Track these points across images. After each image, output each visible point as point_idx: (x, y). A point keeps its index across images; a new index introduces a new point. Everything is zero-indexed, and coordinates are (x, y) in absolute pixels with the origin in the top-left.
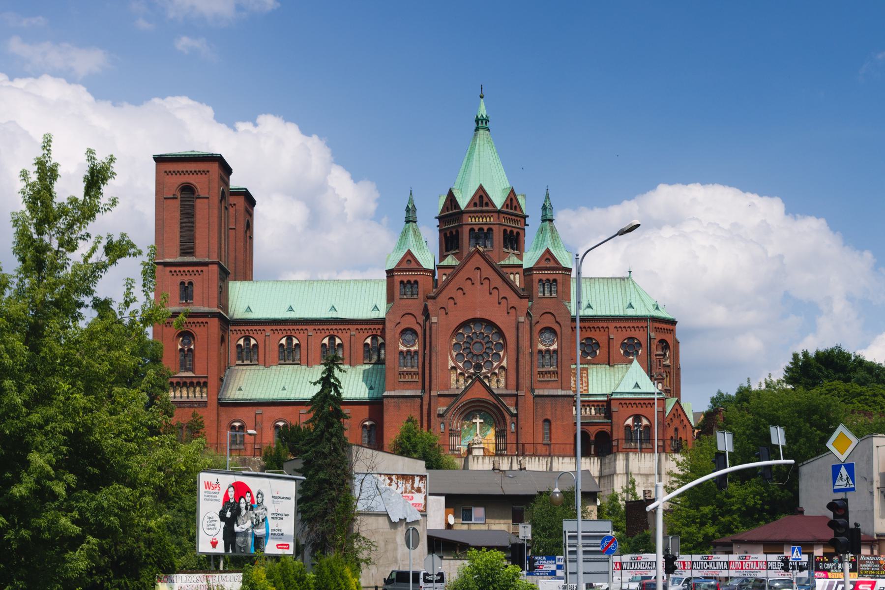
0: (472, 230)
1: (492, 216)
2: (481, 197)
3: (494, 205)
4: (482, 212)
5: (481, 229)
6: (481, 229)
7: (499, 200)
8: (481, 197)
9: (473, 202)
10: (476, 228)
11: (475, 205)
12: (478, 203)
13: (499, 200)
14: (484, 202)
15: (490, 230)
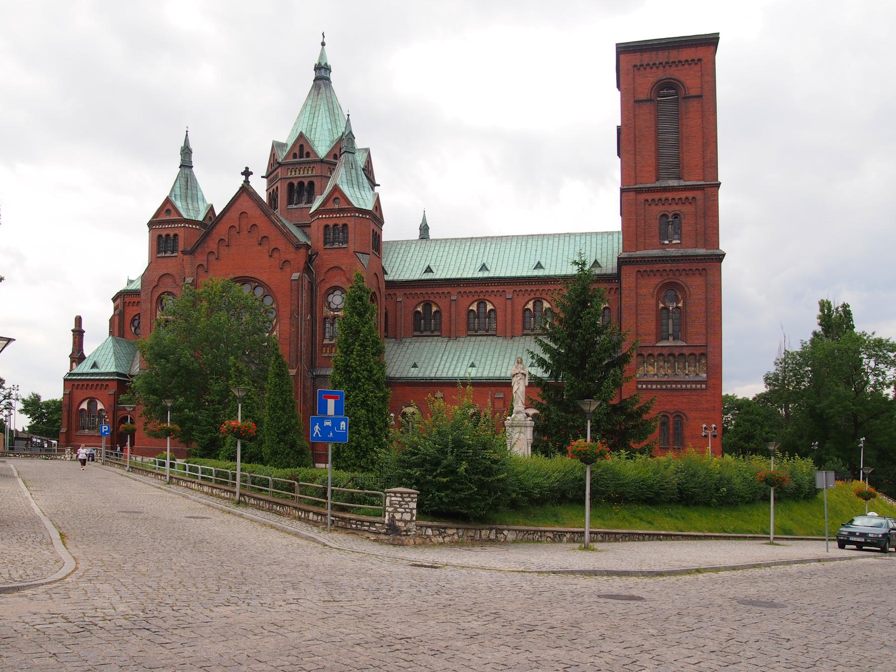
0: (291, 185)
1: (314, 167)
2: (302, 146)
3: (316, 155)
4: (300, 163)
5: (301, 184)
6: (301, 184)
7: (322, 150)
8: (302, 146)
9: (292, 154)
10: (296, 183)
11: (295, 156)
12: (298, 153)
13: (322, 150)
14: (305, 153)
15: (311, 184)
